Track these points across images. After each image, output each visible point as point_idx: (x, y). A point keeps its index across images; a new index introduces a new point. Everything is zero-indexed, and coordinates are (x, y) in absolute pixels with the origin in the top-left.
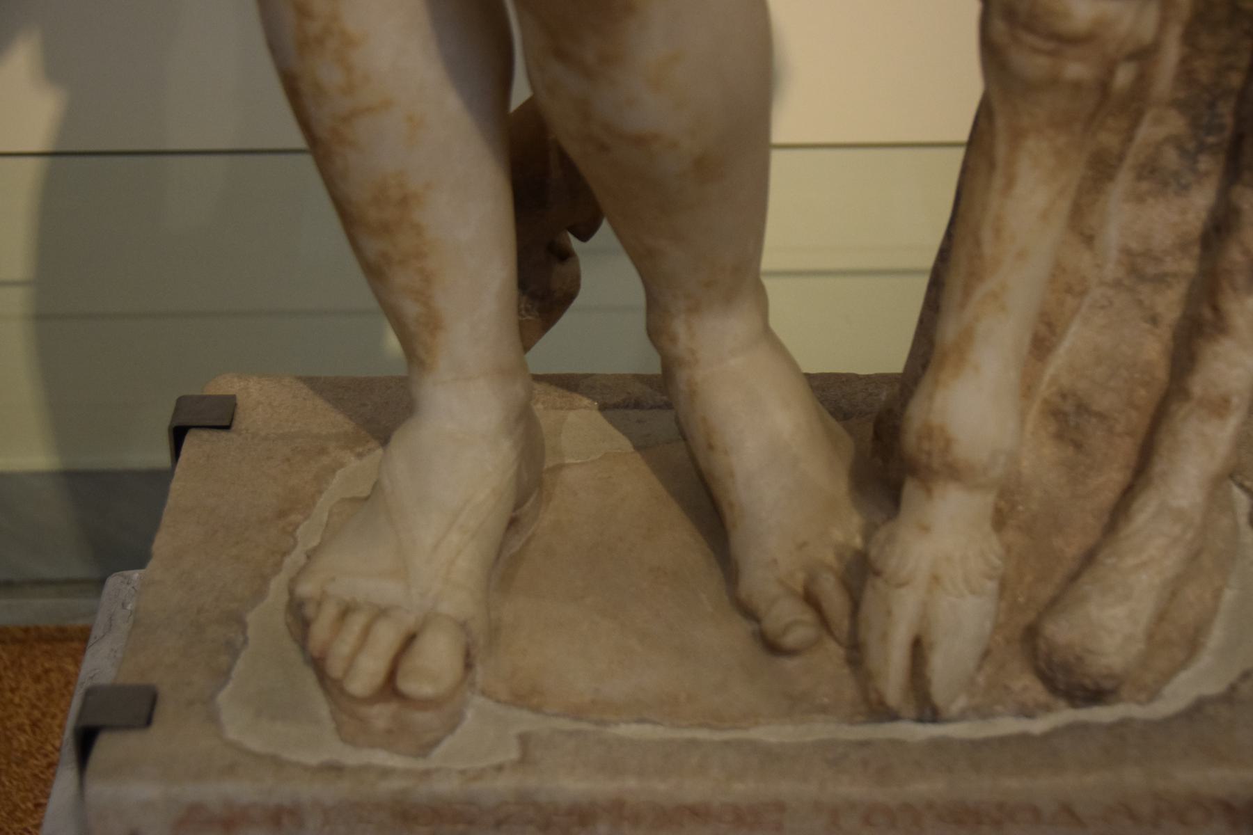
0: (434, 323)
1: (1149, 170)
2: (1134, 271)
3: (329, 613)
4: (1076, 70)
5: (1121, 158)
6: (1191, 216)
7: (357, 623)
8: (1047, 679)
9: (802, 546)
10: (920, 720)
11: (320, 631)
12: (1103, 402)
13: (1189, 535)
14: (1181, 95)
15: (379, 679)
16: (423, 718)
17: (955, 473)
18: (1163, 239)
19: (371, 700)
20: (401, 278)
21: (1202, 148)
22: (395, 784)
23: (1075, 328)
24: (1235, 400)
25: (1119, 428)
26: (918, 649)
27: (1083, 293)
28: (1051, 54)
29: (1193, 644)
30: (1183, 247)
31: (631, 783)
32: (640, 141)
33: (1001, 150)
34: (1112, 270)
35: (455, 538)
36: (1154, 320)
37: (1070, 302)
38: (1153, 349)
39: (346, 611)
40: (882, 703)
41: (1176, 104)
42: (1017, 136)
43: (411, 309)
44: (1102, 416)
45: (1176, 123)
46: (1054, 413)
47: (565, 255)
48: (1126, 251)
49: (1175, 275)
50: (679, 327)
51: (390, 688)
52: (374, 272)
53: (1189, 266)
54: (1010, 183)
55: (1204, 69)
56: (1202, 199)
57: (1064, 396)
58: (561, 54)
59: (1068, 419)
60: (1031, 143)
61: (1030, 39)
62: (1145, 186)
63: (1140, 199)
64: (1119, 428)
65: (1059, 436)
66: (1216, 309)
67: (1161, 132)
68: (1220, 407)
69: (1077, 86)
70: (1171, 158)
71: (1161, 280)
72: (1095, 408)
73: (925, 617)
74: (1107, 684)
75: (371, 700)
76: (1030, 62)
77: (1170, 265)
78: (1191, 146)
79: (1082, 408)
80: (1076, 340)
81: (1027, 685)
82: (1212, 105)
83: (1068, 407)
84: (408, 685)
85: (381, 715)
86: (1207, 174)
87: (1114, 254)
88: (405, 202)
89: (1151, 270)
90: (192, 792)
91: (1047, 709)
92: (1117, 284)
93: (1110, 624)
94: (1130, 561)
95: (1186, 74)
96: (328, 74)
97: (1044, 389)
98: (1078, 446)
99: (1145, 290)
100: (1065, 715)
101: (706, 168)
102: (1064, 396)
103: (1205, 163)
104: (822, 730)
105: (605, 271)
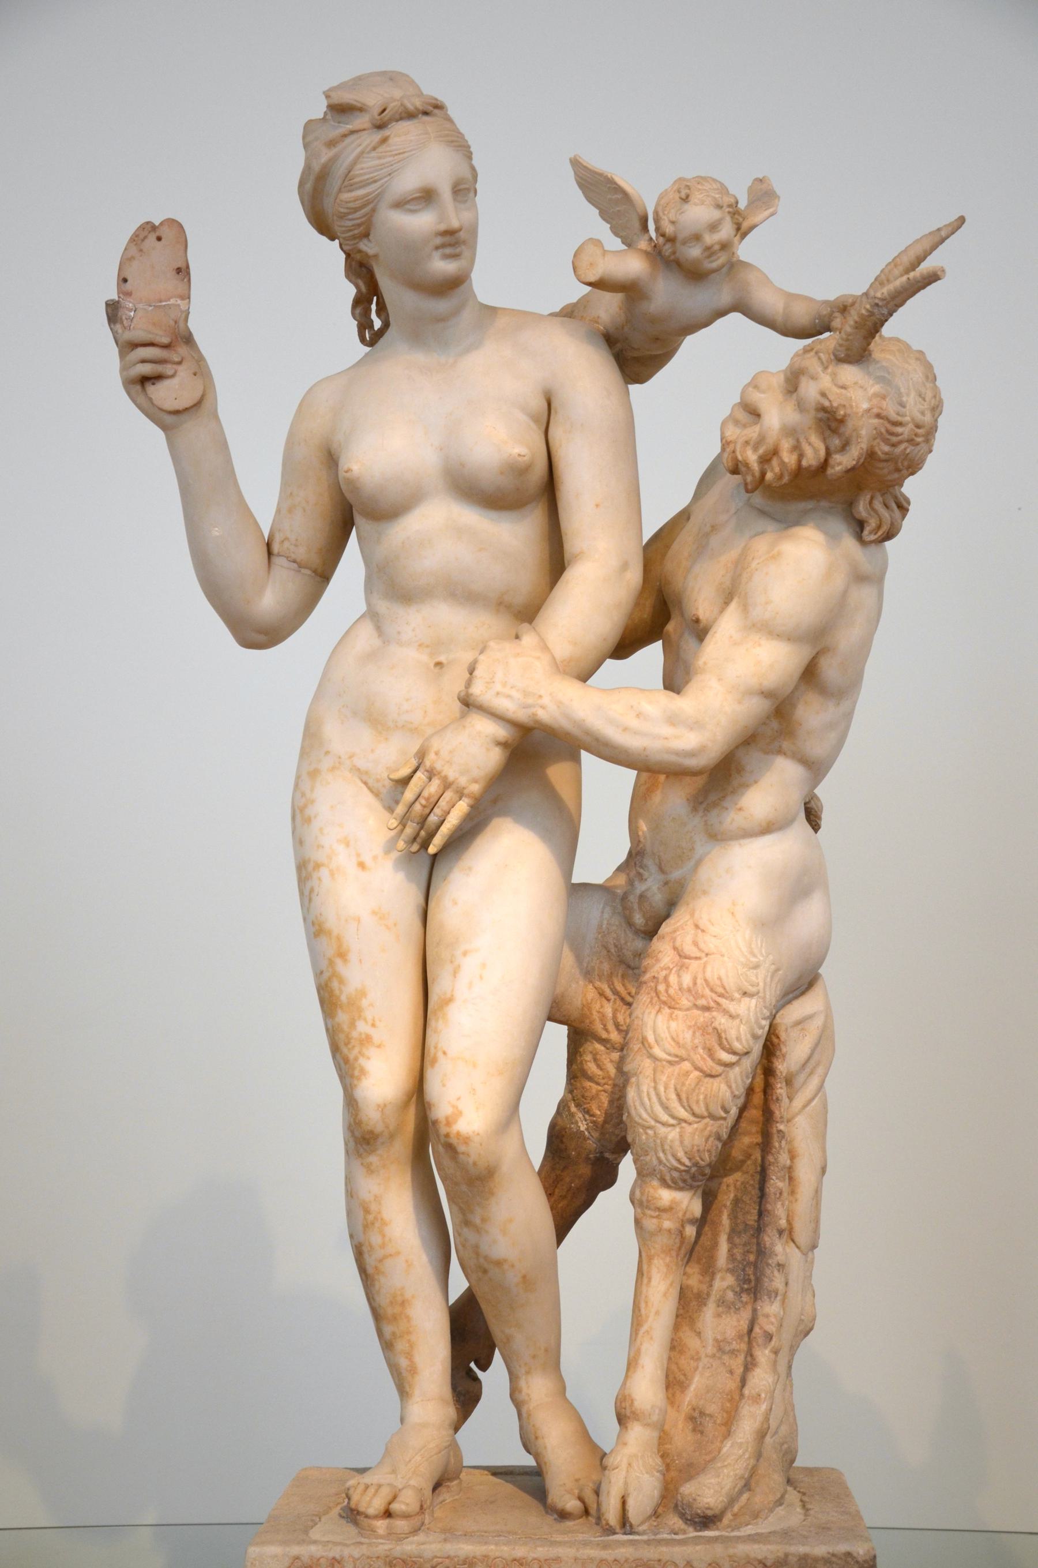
0: (413, 1370)
1: (721, 1302)
2: (720, 1349)
3: (361, 1487)
4: (667, 1224)
5: (708, 1295)
6: (742, 1322)
7: (372, 1490)
8: (682, 1515)
9: (577, 1480)
10: (625, 1534)
11: (355, 1497)
12: (712, 1409)
13: (747, 1456)
14: (731, 1266)
15: (382, 1508)
16: (401, 1525)
17: (636, 1416)
18: (731, 1333)
19: (376, 1517)
20: (400, 1346)
21: (742, 1290)
22: (387, 1547)
23: (696, 1379)
24: (763, 1395)
25: (718, 1422)
26: (624, 1503)
27: (699, 1359)
28: (657, 1217)
29: (756, 1516)
30: (740, 1337)
31: (493, 1547)
32: (499, 1263)
33: (645, 1267)
34: (710, 1349)
35: (418, 1458)
36: (731, 1372)
37: (693, 1364)
38: (732, 1385)
39: (367, 1487)
40: (607, 1524)
41: (728, 1270)
42: (650, 1258)
43: (403, 1362)
44: (711, 1416)
45: (730, 1280)
46: (691, 1419)
47: (476, 1379)
48: (716, 1340)
49: (738, 1351)
50: (522, 1383)
51: (388, 1514)
52: (387, 1345)
53: (744, 1346)
54: (650, 1279)
55: (738, 1252)
56: (746, 1315)
57: (694, 1410)
58: (467, 1223)
59: (696, 1419)
60: (656, 1261)
61: (649, 1212)
62: (720, 1309)
63: (719, 1315)
64: (718, 1422)
65: (694, 1430)
66: (752, 1355)
67: (725, 1284)
68: (756, 1399)
69: (669, 1231)
70: (730, 1295)
71: (733, 1353)
72: (707, 1412)
73: (626, 1484)
74: (709, 1513)
75: (376, 1517)
76: (650, 1224)
77: (735, 1345)
78: (738, 1289)
79: (702, 1414)
80: (697, 1383)
81: (674, 1521)
82: (744, 1270)
83: (696, 1414)
84: (396, 1507)
85: (381, 1525)
86: (746, 1303)
87: (711, 1342)
88: (403, 1303)
89: (727, 1348)
90: (295, 1550)
91: (685, 1532)
92: (714, 1356)
93: (708, 1491)
94: (719, 1465)
95: (731, 1256)
96: (375, 1239)
97: (685, 1408)
98: (702, 1433)
99: (726, 1358)
100: (692, 1533)
101: (526, 1281)
102: (694, 1410)
103: (745, 1298)
104: (580, 1537)
105: (494, 1379)
